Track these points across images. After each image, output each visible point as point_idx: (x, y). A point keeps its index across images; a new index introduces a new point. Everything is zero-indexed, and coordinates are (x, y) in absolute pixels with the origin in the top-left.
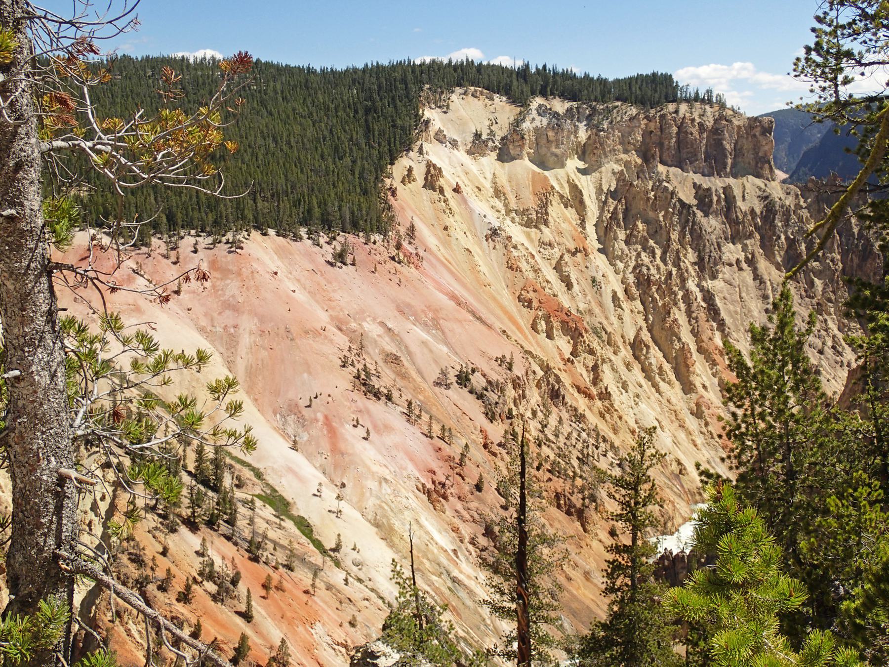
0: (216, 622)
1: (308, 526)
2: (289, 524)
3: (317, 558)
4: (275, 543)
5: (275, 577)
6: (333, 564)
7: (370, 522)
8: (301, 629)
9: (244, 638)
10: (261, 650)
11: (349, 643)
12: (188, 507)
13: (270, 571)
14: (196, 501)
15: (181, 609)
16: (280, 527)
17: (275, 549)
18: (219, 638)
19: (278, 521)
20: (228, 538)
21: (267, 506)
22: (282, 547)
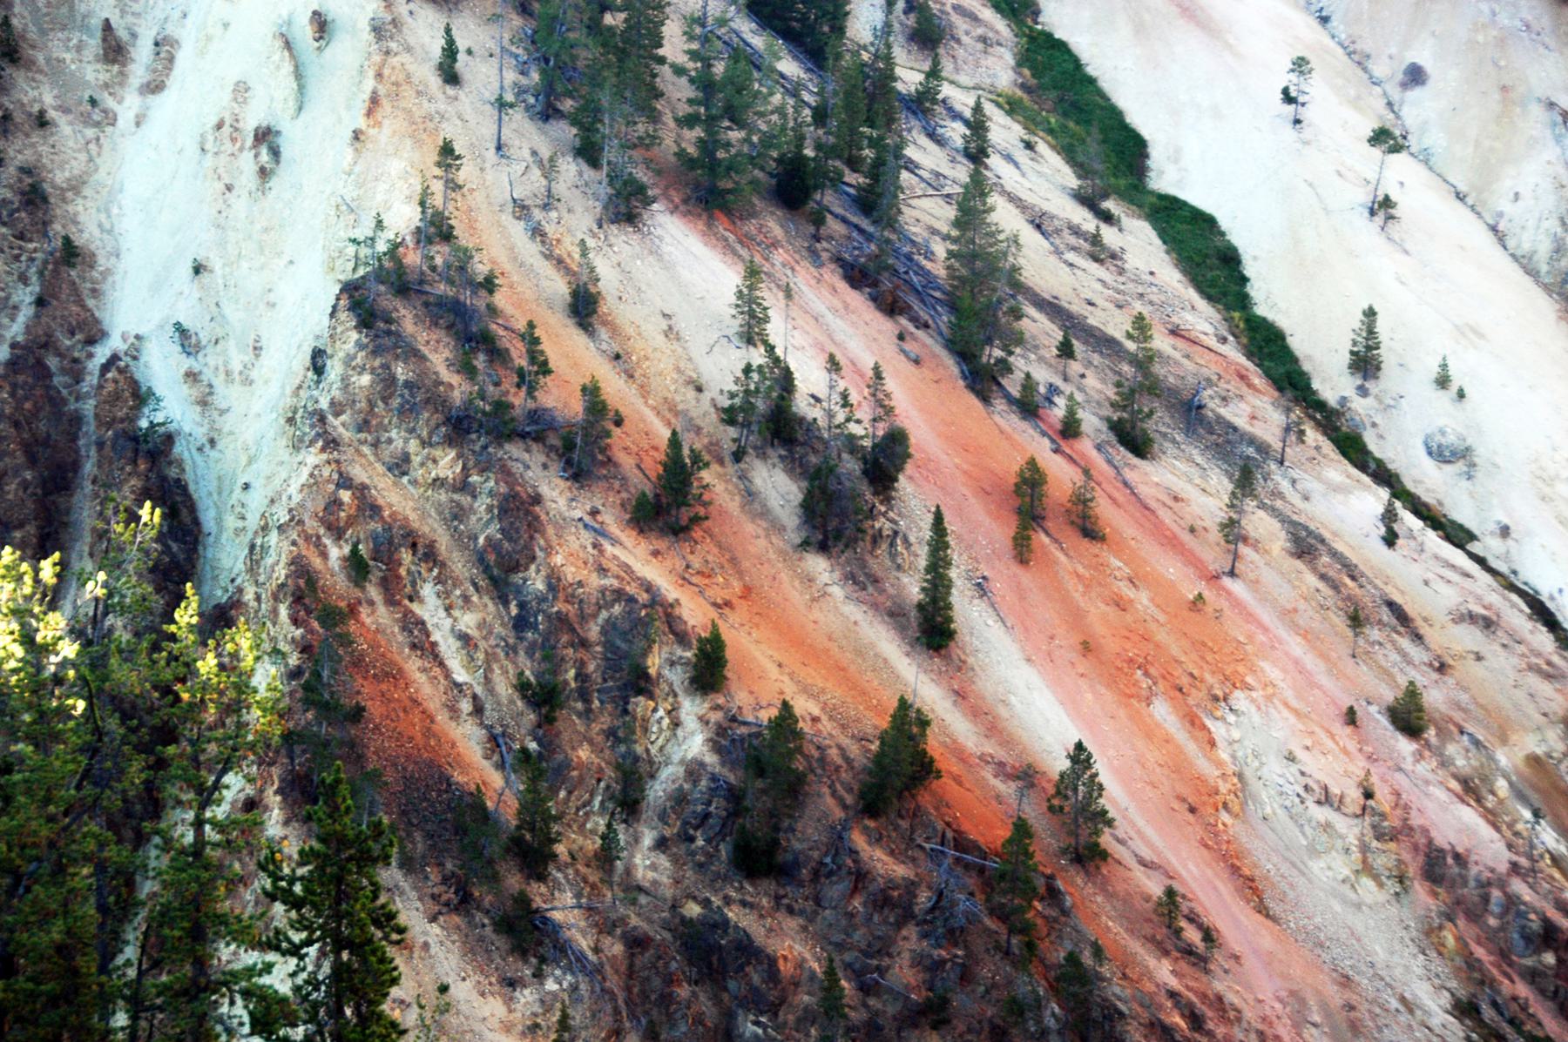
0: (794, 639)
1: (1230, 259)
2: (1138, 240)
3: (1256, 411)
4: (1076, 332)
5: (1061, 474)
6: (1328, 447)
7: (1526, 265)
8: (1162, 711)
9: (908, 724)
10: (984, 785)
11: (1383, 799)
12: (689, 121)
13: (1041, 448)
14: (722, 98)
15: (643, 562)
16: (1099, 252)
17: (1066, 351)
18: (803, 706)
19: (1089, 222)
20: (857, 276)
21: (1042, 147)
22: (1103, 343)
